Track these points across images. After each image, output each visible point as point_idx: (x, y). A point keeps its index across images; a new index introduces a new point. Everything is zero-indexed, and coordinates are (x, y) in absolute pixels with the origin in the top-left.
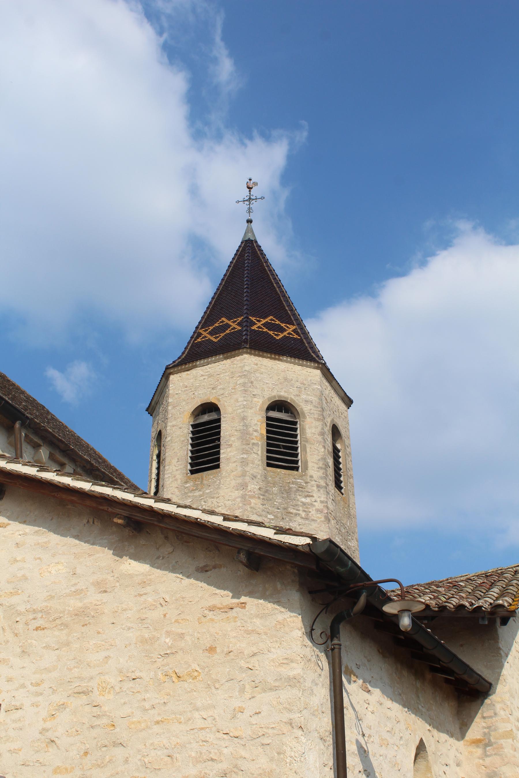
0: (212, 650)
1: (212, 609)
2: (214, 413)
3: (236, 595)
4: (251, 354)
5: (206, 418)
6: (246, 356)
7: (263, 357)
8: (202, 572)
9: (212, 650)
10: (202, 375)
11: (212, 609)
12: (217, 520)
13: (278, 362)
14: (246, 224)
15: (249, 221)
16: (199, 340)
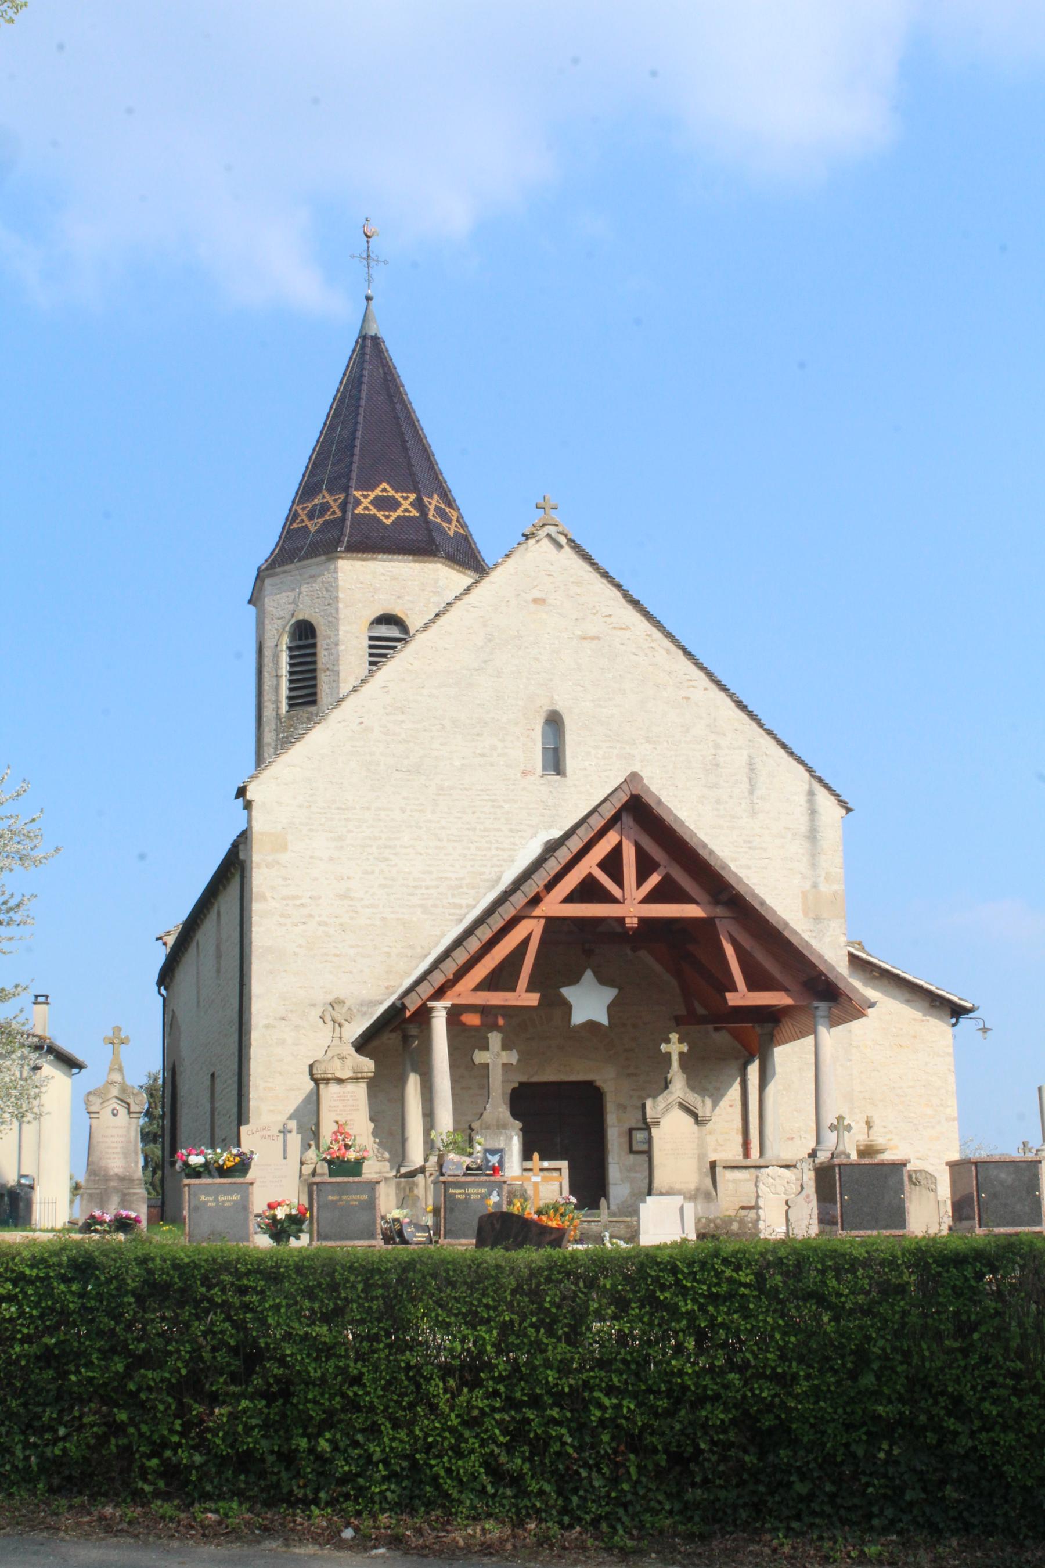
0: (915, 1037)
1: (915, 1020)
2: (394, 628)
3: (924, 1015)
4: (444, 564)
5: (384, 631)
6: (439, 566)
7: (453, 568)
8: (907, 1002)
9: (915, 1037)
10: (383, 574)
11: (915, 1020)
12: (932, 988)
13: (462, 576)
14: (365, 302)
15: (369, 299)
16: (359, 510)
